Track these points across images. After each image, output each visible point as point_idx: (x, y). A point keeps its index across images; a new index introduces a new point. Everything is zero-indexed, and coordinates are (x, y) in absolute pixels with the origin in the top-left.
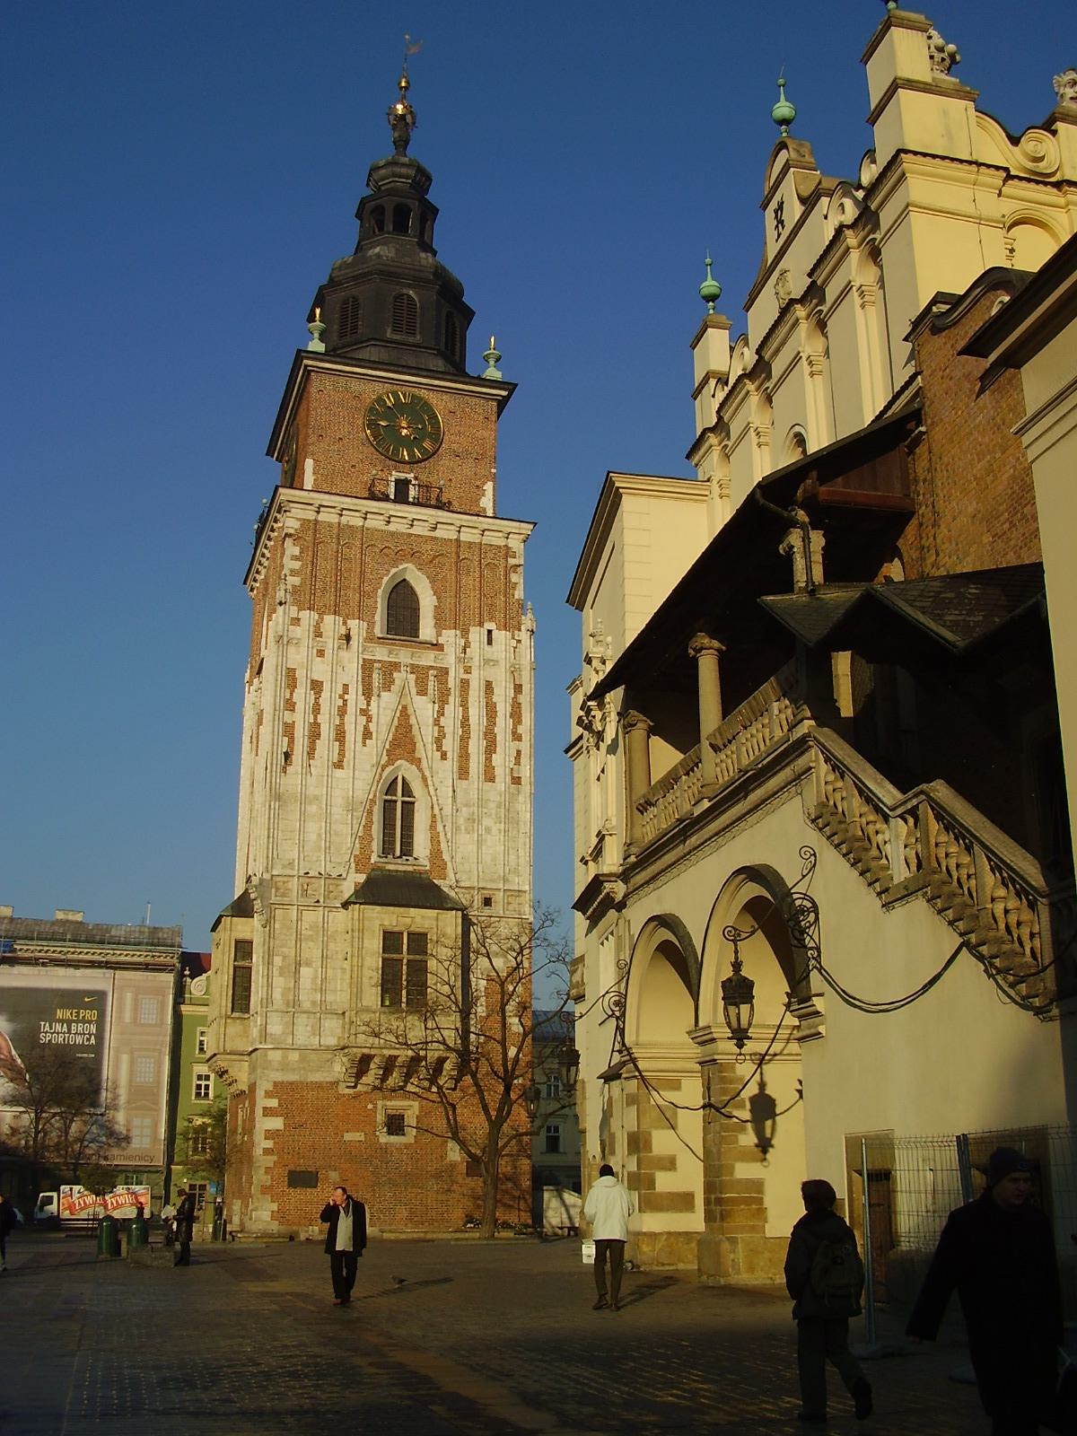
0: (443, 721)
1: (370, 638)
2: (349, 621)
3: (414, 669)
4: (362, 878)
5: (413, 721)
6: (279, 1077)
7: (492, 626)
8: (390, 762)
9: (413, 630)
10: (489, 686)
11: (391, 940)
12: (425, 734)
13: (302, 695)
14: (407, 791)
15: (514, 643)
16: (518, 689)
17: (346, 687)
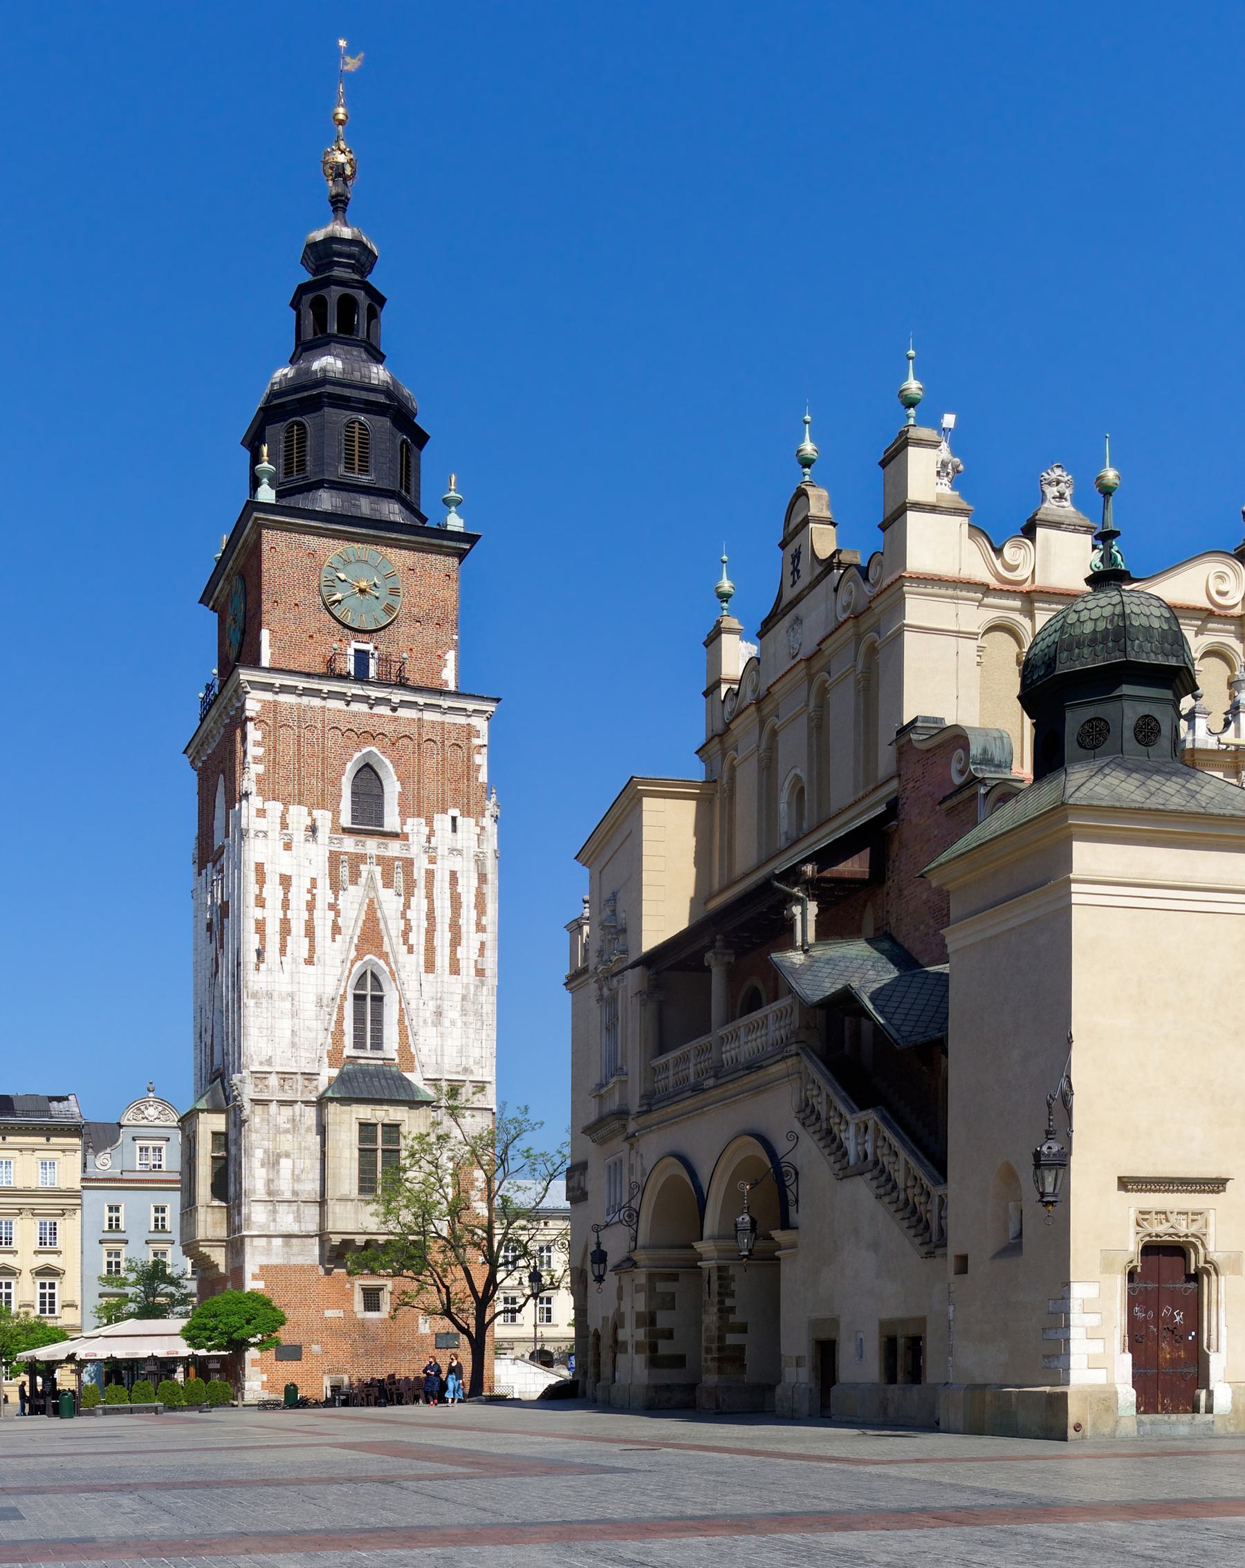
0: (409, 914)
2: (315, 812)
4: (335, 1072)
6: (265, 1261)
7: (455, 812)
9: (379, 820)
10: (453, 876)
12: (394, 927)
15: (478, 830)
16: (482, 878)
17: (314, 881)
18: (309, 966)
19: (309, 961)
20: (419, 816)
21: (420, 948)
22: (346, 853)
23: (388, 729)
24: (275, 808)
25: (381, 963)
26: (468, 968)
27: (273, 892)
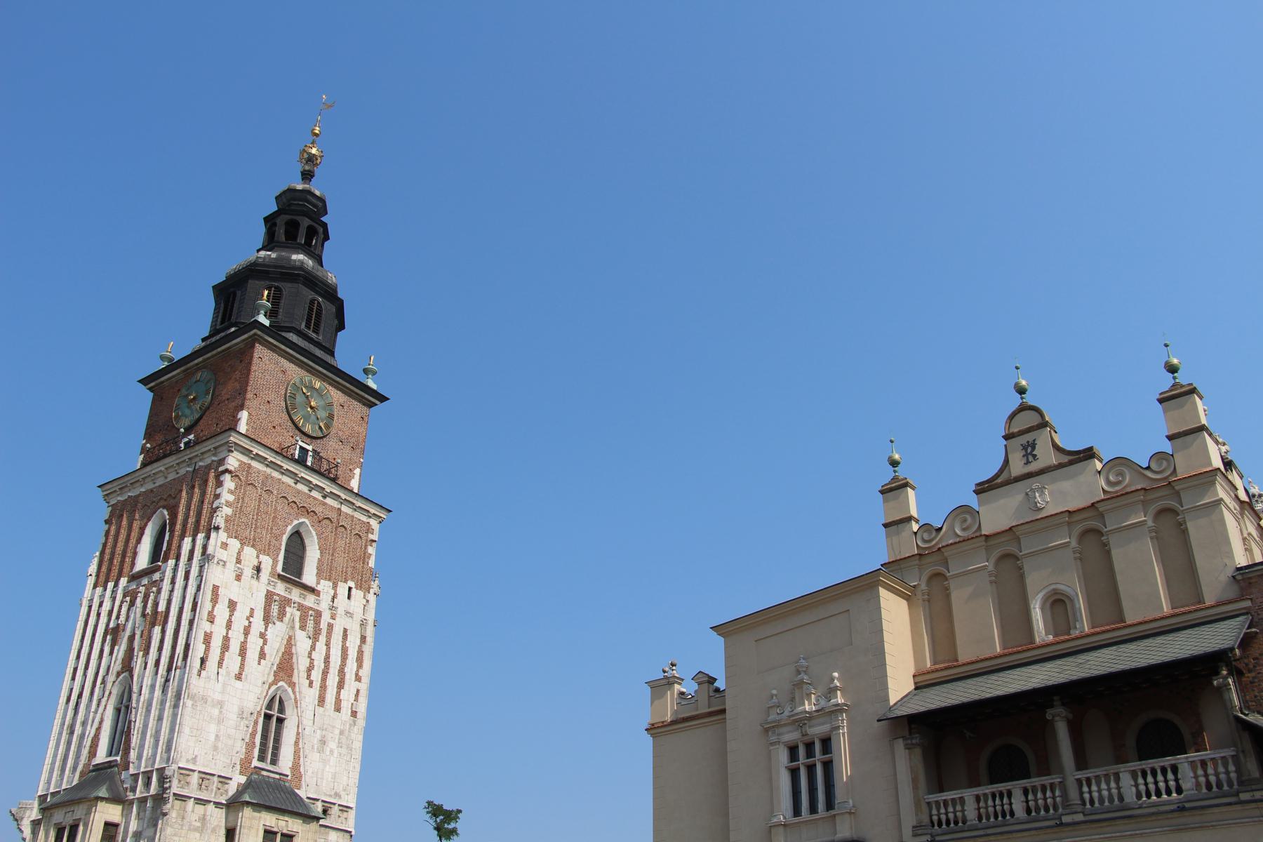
0: (314, 655)
2: (261, 556)
3: (301, 607)
4: (243, 779)
7: (351, 584)
8: (275, 682)
9: (299, 573)
12: (301, 663)
16: (363, 639)
18: (237, 681)
20: (329, 580)
21: (317, 684)
22: (278, 595)
23: (319, 509)
24: (235, 544)
25: (290, 690)
26: (346, 707)
27: (222, 611)
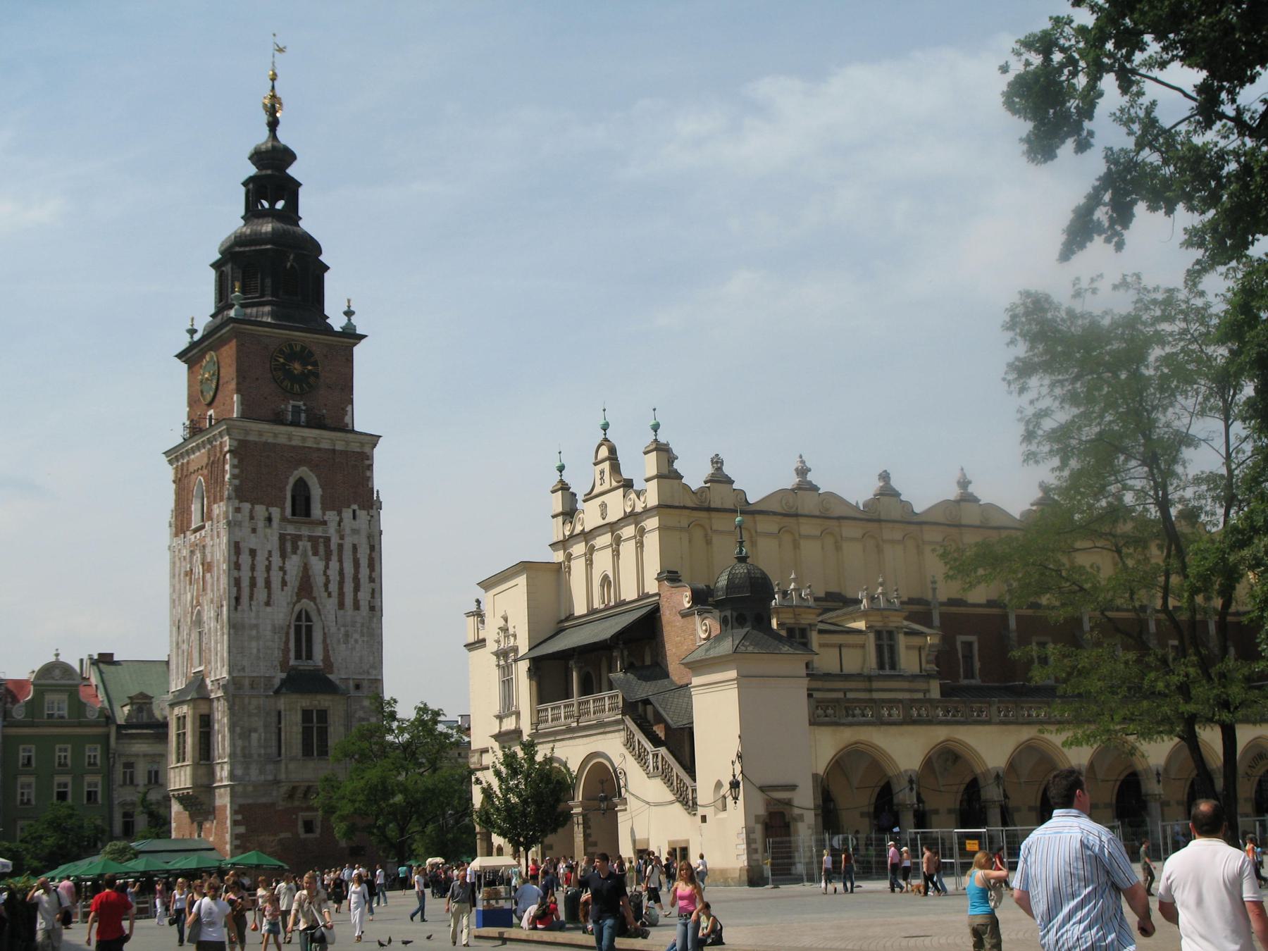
0: (329, 572)
1: (283, 519)
3: (311, 538)
4: (284, 675)
5: (310, 573)
7: (355, 507)
8: (298, 601)
9: (307, 513)
10: (355, 548)
11: (307, 715)
12: (319, 580)
13: (245, 559)
14: (308, 619)
15: (369, 518)
17: (270, 552)
19: (268, 604)
20: (334, 510)
21: (335, 594)
22: (289, 534)
24: (246, 506)
25: (312, 604)
26: (364, 605)
